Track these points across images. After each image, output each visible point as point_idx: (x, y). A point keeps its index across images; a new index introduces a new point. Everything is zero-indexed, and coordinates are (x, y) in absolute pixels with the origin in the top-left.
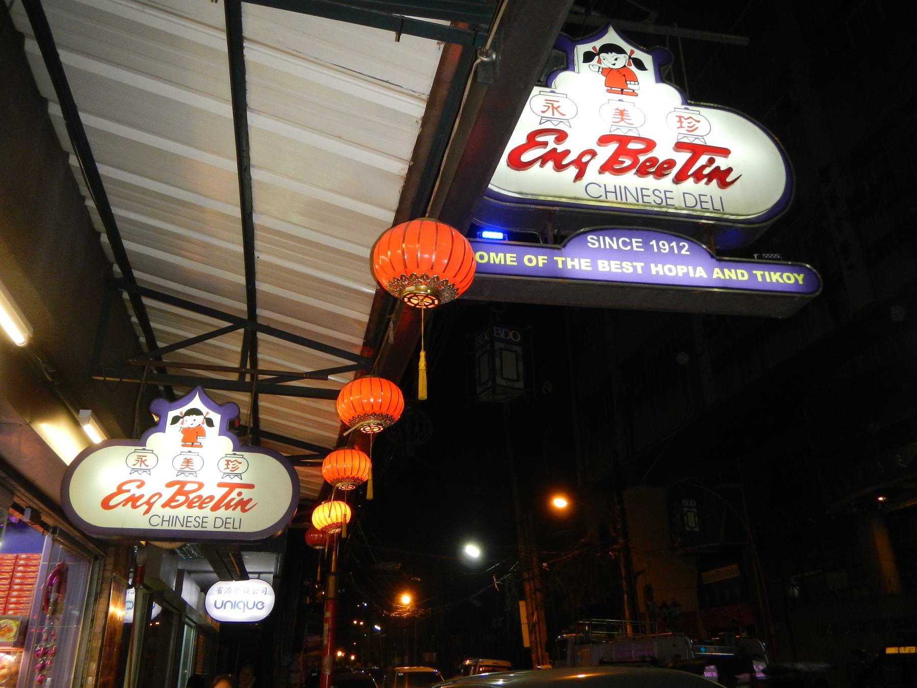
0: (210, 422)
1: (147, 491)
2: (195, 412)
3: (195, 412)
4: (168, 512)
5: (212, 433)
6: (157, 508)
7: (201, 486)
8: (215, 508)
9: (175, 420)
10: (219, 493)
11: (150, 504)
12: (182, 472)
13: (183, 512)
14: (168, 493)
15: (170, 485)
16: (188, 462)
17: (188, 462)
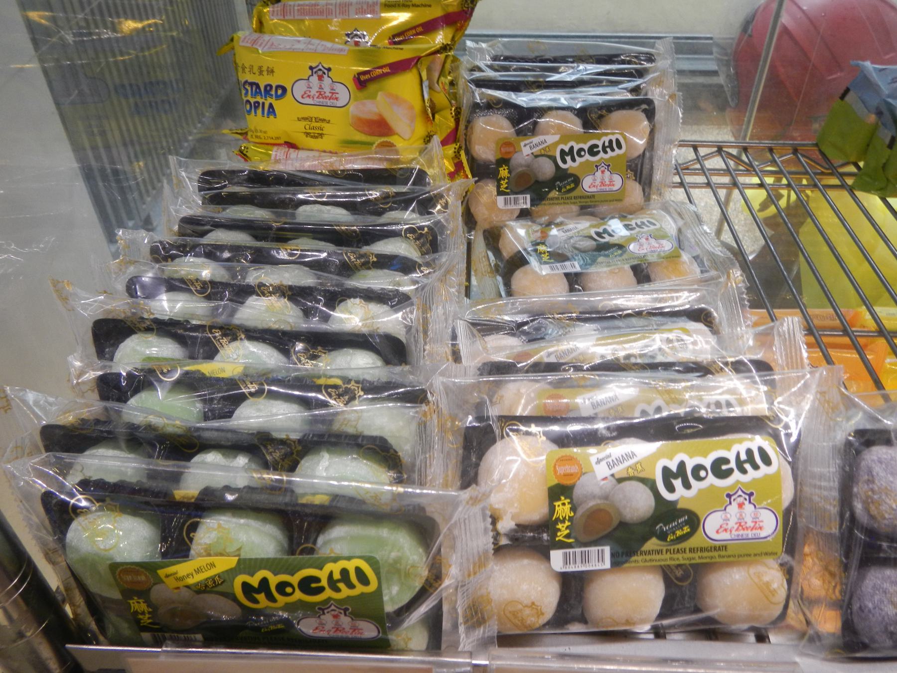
0: (746, 499)
1: (729, 527)
2: (740, 496)
3: (740, 496)
4: (737, 533)
5: (747, 503)
6: (733, 532)
7: (746, 523)
8: (752, 529)
9: (734, 500)
10: (752, 525)
11: (731, 531)
12: (739, 519)
13: (741, 532)
14: (736, 527)
15: (736, 523)
16: (741, 515)
17: (741, 515)
